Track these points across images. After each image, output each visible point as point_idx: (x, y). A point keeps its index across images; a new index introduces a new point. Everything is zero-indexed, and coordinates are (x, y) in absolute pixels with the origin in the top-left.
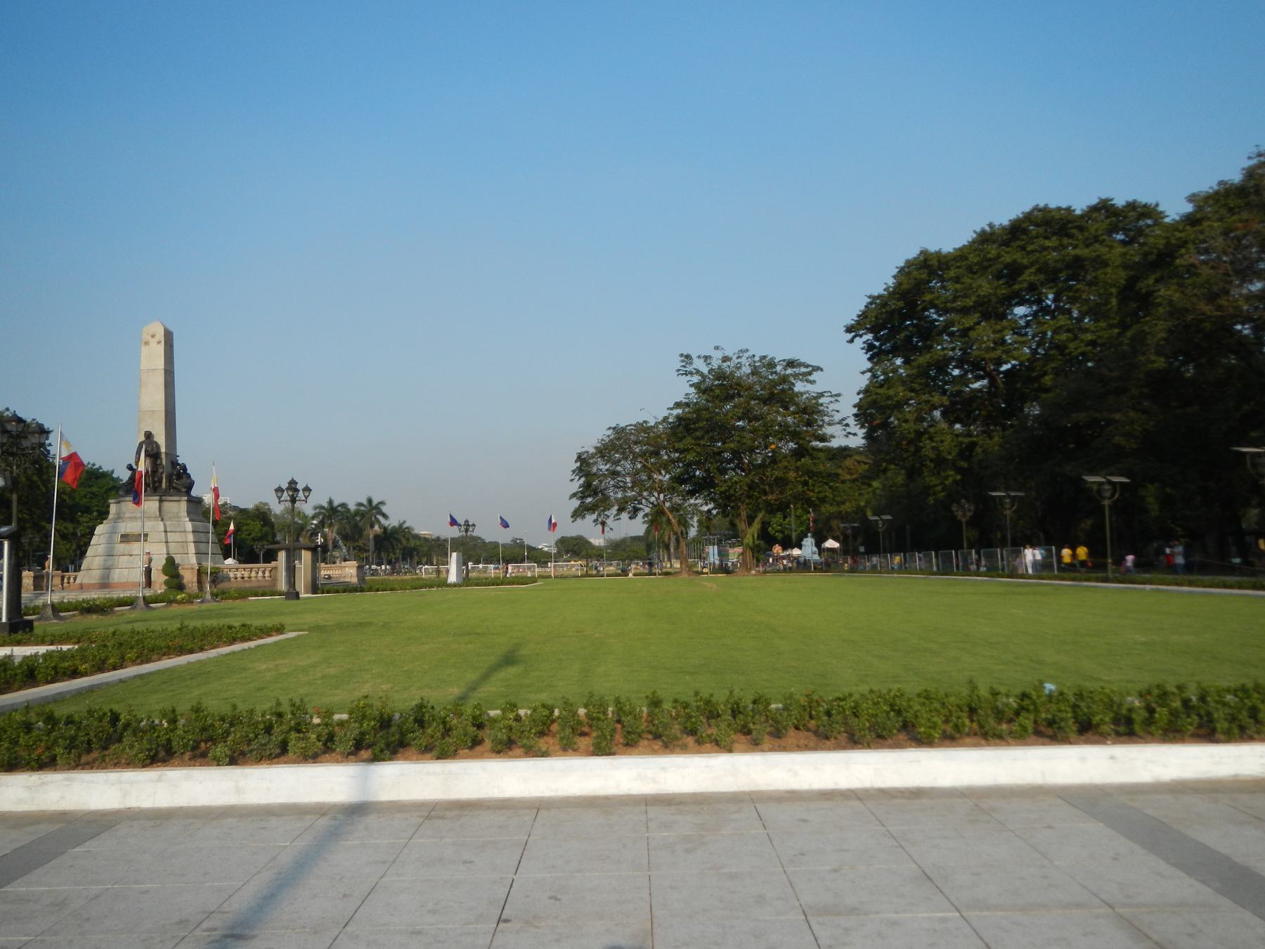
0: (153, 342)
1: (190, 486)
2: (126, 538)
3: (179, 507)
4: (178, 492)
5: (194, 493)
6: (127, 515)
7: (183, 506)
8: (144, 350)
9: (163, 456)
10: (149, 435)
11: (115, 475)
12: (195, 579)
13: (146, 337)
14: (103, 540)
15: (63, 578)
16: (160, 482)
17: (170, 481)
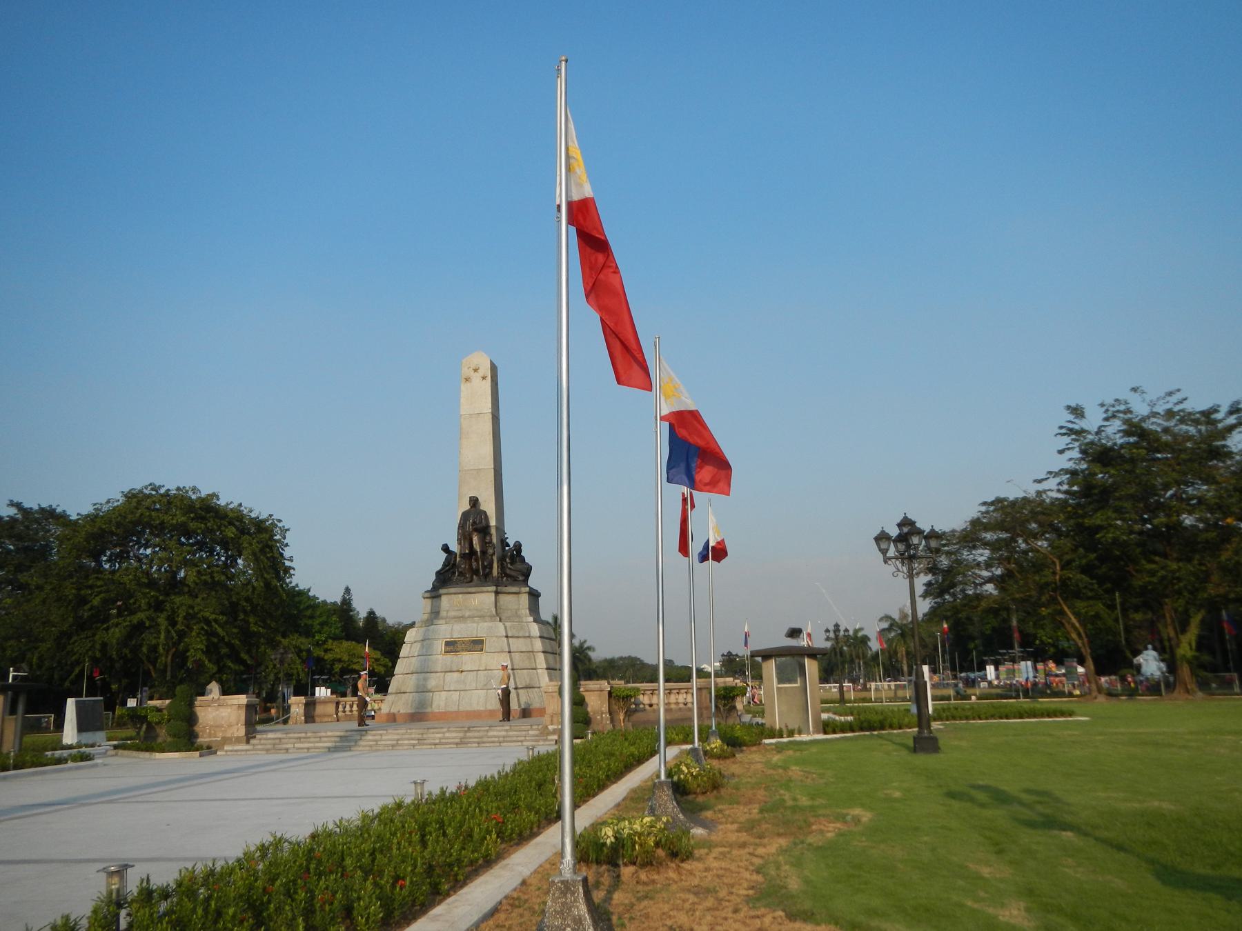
0: (476, 378)
1: (527, 572)
2: (452, 646)
3: (517, 602)
4: (514, 580)
5: (532, 582)
6: (452, 614)
7: (524, 599)
8: (464, 387)
9: (493, 531)
10: (474, 502)
11: (311, 594)
12: (605, 708)
13: (466, 372)
14: (416, 649)
15: (338, 704)
16: (491, 568)
17: (502, 567)
